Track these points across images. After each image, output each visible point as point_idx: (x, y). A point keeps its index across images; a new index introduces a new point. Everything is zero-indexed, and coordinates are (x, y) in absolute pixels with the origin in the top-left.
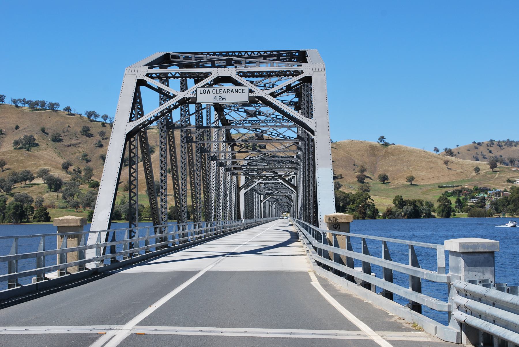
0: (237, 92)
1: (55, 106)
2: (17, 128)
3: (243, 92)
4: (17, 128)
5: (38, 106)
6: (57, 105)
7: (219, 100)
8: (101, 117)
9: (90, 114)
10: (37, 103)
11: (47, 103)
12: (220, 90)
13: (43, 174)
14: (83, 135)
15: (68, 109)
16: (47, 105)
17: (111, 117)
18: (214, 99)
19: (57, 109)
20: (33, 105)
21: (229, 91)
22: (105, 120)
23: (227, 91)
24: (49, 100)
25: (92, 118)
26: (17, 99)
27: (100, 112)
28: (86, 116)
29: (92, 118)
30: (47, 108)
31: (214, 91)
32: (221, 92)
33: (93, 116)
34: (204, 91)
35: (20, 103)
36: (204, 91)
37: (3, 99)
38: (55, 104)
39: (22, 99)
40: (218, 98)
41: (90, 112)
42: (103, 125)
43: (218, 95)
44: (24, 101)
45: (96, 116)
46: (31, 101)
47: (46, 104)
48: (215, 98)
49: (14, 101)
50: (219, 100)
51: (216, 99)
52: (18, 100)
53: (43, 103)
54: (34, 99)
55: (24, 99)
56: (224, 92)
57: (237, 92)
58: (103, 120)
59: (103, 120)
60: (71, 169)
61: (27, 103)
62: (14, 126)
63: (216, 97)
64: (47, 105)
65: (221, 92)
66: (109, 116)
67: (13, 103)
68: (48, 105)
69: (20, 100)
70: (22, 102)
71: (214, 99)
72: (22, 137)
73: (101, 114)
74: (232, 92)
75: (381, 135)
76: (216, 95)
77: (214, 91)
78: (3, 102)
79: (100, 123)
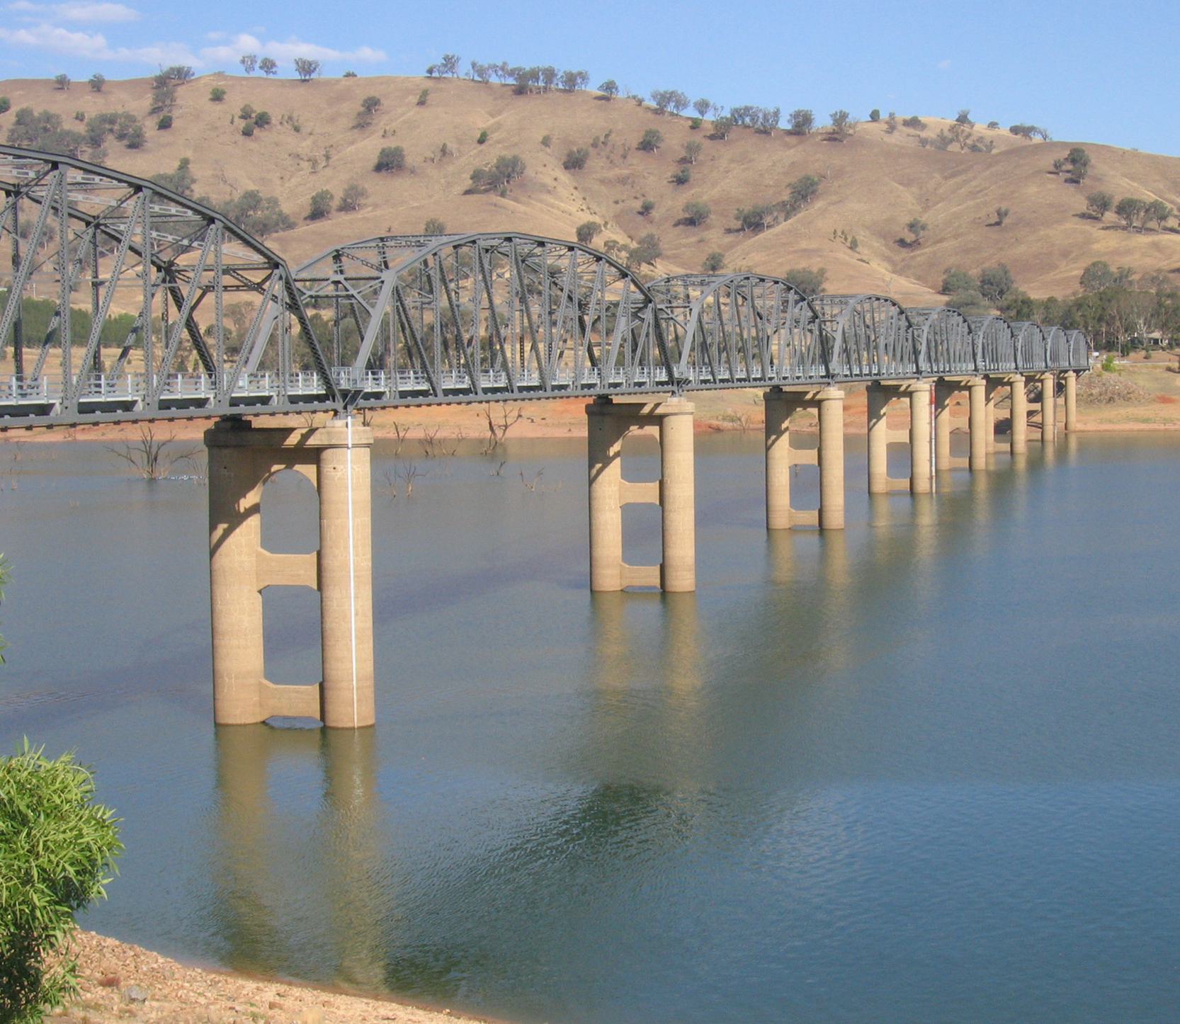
1: (579, 81)
5: (537, 80)
6: (583, 76)
8: (692, 104)
9: (664, 99)
10: (534, 75)
11: (560, 74)
16: (559, 77)
17: (719, 106)
22: (702, 113)
24: (562, 68)
26: (487, 66)
27: (693, 96)
35: (494, 75)
37: (453, 66)
38: (580, 74)
39: (500, 64)
41: (666, 92)
42: (695, 125)
45: (681, 103)
46: (520, 69)
47: (556, 75)
49: (481, 71)
52: (490, 67)
53: (550, 74)
54: (527, 66)
55: (505, 64)
58: (696, 115)
64: (559, 77)
66: (711, 103)
67: (478, 75)
68: (562, 77)
69: (494, 68)
70: (500, 73)
75: (705, 98)
78: (453, 73)
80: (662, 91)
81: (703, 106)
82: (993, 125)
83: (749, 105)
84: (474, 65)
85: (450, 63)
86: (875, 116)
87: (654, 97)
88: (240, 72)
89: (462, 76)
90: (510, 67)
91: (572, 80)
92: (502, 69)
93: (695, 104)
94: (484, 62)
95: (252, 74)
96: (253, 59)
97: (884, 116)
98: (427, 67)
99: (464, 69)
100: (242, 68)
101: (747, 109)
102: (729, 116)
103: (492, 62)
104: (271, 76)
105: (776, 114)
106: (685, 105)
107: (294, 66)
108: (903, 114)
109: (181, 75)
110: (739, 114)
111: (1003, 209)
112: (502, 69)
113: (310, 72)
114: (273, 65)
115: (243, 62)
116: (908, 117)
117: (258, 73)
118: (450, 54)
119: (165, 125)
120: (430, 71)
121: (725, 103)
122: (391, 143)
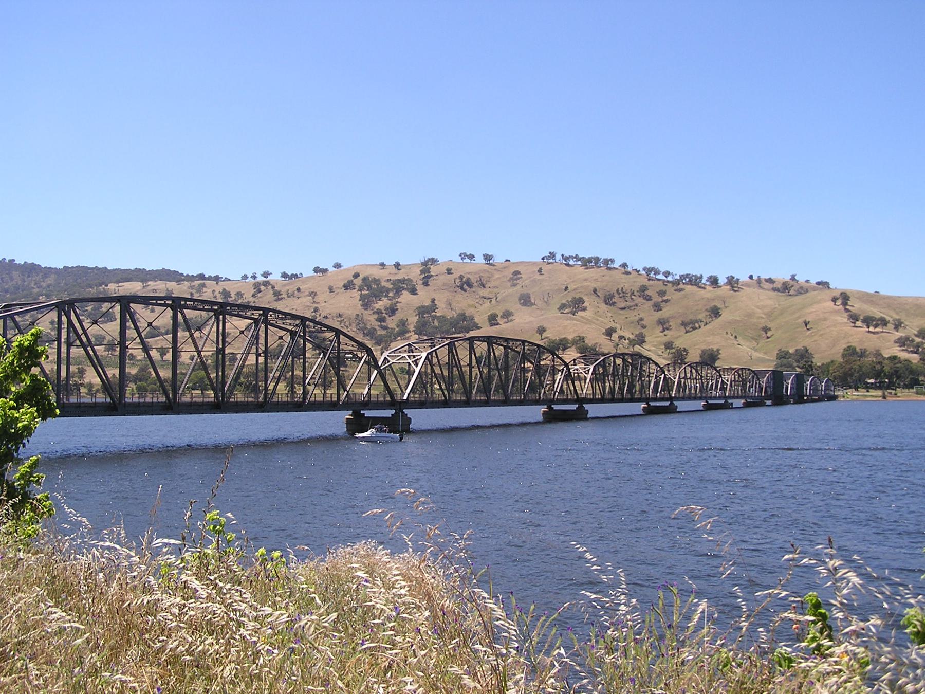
1: (610, 263)
2: (566, 288)
4: (566, 288)
5: (591, 262)
6: (612, 261)
9: (648, 270)
10: (590, 260)
14: (640, 296)
15: (624, 265)
17: (674, 273)
19: (612, 266)
20: (587, 263)
22: (666, 277)
24: (603, 256)
25: (652, 275)
27: (662, 270)
33: (653, 273)
35: (572, 260)
38: (610, 259)
39: (574, 256)
44: (577, 258)
46: (583, 258)
49: (566, 259)
53: (597, 259)
55: (577, 255)
58: (664, 278)
59: (664, 278)
60: (615, 336)
61: (580, 259)
69: (572, 257)
72: (570, 299)
73: (662, 270)
79: (661, 282)
80: (648, 267)
81: (667, 274)
82: (807, 281)
83: (688, 273)
84: (563, 255)
85: (552, 255)
86: (751, 277)
90: (580, 256)
91: (607, 262)
93: (663, 273)
94: (566, 255)
95: (465, 261)
97: (755, 278)
98: (542, 257)
99: (558, 257)
101: (687, 275)
102: (679, 278)
103: (571, 255)
104: (472, 261)
105: (701, 277)
107: (483, 258)
108: (764, 276)
109: (433, 261)
110: (683, 277)
111: (807, 320)
114: (474, 257)
115: (460, 255)
116: (767, 277)
118: (552, 251)
119: (426, 284)
120: (543, 259)
121: (678, 271)
122: (525, 291)
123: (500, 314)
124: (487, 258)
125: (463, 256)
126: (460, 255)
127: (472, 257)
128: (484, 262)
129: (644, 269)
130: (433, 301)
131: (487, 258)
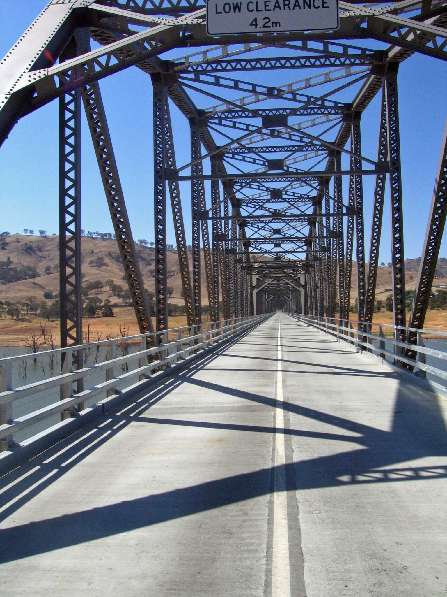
0: (309, 7)
2: (92, 252)
3: (325, 5)
7: (264, 27)
10: (105, 235)
12: (267, 4)
13: (110, 283)
18: (251, 25)
21: (288, 5)
22: (152, 245)
23: (285, 5)
28: (139, 243)
29: (143, 244)
30: (113, 238)
31: (252, 7)
32: (267, 8)
34: (227, 7)
36: (227, 7)
39: (96, 232)
40: (261, 23)
43: (260, 17)
45: (146, 243)
46: (101, 233)
48: (254, 23)
49: (91, 234)
50: (264, 27)
51: (256, 25)
52: (93, 233)
54: (104, 232)
56: (275, 7)
57: (309, 7)
61: (99, 234)
62: (90, 251)
63: (256, 20)
65: (267, 8)
69: (94, 233)
71: (251, 25)
72: (96, 258)
74: (295, 6)
76: (254, 14)
77: (252, 7)
84: (89, 232)
87: (139, 241)
88: (23, 233)
89: (85, 235)
92: (97, 233)
94: (91, 231)
96: (27, 230)
100: (24, 232)
106: (147, 243)
107: (39, 232)
112: (97, 233)
113: (43, 234)
114: (33, 232)
115: (24, 231)
117: (28, 234)
123: (52, 267)
124: (42, 232)
125: (26, 231)
126: (24, 231)
127: (31, 232)
128: (39, 235)
129: (139, 241)
130: (9, 258)
131: (42, 232)
